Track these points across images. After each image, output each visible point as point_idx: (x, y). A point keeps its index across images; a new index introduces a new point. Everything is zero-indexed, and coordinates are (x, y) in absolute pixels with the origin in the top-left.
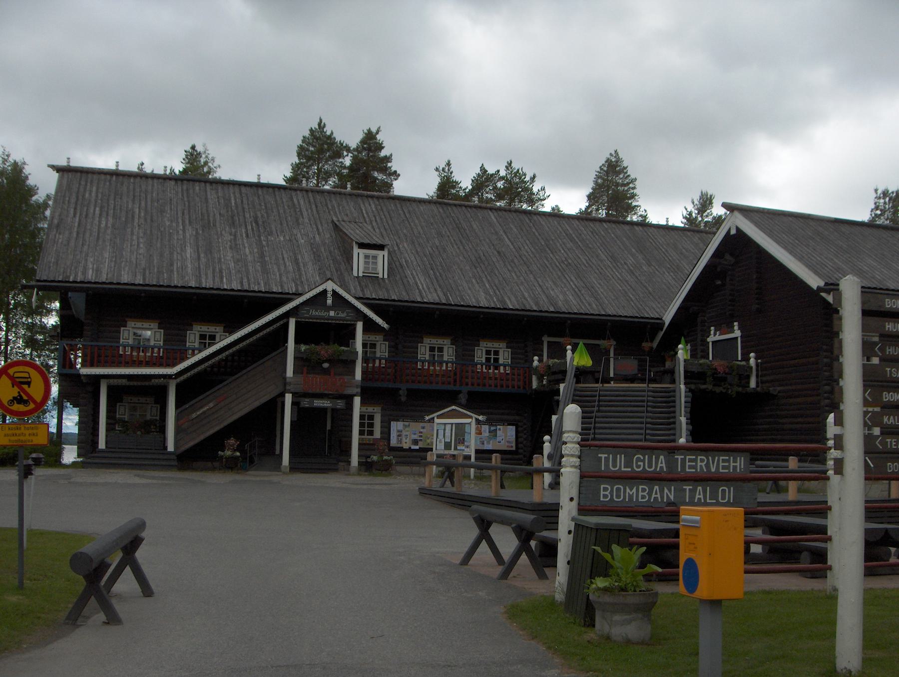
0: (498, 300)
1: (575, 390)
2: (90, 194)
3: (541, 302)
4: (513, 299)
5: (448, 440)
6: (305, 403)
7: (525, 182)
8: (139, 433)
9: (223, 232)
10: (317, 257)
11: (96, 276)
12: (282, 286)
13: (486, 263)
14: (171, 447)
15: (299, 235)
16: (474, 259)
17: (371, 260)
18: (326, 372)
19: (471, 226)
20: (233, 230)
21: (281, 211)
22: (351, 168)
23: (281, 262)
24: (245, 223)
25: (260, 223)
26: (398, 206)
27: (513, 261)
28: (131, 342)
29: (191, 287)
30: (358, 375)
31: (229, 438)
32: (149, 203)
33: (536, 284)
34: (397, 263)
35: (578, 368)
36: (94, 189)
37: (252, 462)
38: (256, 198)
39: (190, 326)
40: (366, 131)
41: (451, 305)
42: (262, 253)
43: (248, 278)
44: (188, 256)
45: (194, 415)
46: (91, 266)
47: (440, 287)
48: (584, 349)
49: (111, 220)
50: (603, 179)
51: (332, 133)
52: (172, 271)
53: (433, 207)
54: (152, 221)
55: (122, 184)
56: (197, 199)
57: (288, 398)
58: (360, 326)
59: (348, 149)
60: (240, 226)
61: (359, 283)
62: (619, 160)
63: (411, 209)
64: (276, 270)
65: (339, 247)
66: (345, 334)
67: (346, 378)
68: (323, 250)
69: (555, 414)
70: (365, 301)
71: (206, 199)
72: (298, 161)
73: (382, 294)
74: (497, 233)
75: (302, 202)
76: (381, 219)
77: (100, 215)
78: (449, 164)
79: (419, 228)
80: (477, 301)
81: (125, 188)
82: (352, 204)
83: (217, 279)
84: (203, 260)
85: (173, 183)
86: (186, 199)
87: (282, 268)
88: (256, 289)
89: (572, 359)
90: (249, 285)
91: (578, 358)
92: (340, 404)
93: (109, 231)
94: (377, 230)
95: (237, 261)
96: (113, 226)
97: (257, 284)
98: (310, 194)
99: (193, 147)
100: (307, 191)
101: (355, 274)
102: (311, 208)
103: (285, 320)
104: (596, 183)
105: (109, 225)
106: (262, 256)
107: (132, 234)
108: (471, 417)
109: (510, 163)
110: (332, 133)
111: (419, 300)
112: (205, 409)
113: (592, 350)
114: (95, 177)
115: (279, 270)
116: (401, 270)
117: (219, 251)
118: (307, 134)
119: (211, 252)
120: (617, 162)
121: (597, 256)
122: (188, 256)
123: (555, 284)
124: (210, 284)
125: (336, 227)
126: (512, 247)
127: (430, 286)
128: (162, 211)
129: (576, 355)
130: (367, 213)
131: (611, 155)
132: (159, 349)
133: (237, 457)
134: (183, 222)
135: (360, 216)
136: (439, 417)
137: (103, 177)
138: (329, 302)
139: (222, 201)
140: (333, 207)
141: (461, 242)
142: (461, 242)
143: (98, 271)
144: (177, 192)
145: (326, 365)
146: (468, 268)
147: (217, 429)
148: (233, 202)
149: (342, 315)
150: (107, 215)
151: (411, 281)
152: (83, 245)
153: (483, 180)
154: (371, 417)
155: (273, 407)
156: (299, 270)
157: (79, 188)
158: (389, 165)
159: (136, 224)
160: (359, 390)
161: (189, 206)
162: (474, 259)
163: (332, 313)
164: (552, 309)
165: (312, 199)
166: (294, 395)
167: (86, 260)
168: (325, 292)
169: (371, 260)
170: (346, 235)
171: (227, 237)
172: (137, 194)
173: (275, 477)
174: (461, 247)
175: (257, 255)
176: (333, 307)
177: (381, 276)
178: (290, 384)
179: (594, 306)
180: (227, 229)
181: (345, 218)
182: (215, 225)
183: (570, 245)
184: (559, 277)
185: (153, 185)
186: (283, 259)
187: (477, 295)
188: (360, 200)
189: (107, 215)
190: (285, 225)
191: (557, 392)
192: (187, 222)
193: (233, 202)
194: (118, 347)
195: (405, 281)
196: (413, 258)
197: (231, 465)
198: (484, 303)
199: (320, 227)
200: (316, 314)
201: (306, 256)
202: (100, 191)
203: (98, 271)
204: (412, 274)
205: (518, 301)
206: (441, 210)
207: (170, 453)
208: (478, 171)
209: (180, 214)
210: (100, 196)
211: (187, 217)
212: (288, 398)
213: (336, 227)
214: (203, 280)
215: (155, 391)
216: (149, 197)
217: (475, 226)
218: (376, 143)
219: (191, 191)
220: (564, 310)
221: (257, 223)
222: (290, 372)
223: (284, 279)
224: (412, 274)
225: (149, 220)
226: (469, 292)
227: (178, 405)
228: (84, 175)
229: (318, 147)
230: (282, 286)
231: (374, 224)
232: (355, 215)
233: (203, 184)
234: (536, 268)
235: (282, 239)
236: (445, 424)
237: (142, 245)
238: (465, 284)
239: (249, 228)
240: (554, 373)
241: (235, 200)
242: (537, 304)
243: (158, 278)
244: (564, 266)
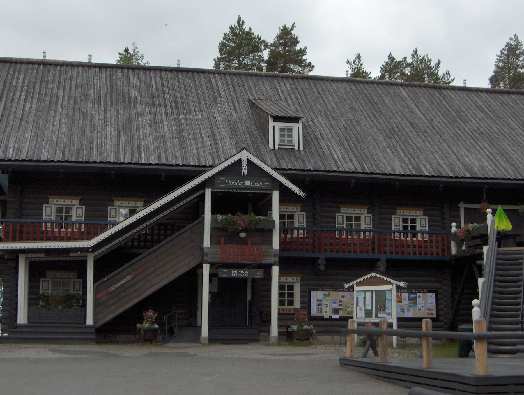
0: (414, 168)
1: (498, 254)
2: (17, 81)
3: (457, 169)
4: (428, 166)
5: (369, 308)
6: (223, 273)
7: (431, 68)
8: (60, 307)
9: (144, 112)
10: (234, 132)
11: (17, 155)
12: (199, 160)
13: (400, 134)
14: (90, 321)
15: (217, 113)
16: (387, 130)
17: (286, 133)
18: (243, 241)
19: (384, 101)
20: (153, 110)
21: (200, 92)
22: (268, 62)
23: (199, 137)
24: (165, 103)
25: (179, 103)
26: (312, 85)
27: (425, 131)
28: (53, 218)
29: (109, 163)
30: (276, 245)
31: (147, 310)
32: (73, 88)
33: (450, 152)
34: (312, 136)
35: (499, 233)
36: (22, 76)
37: (171, 331)
38: (176, 82)
39: (111, 202)
40: (281, 28)
41: (367, 173)
42: (180, 129)
43: (166, 152)
44: (108, 134)
45: (112, 288)
46: (12, 145)
47: (355, 156)
48: (503, 213)
49: (35, 103)
50: (504, 63)
51: (250, 29)
52: (91, 148)
53: (346, 85)
54: (75, 103)
55: (49, 72)
56: (120, 83)
57: (206, 269)
58: (276, 195)
59: (266, 46)
60: (160, 106)
61: (276, 155)
62: (518, 44)
63: (325, 87)
64: (194, 145)
65: (255, 123)
66: (260, 203)
67: (264, 247)
68: (240, 126)
69: (481, 276)
70: (282, 172)
71: (128, 83)
72: (220, 57)
73: (299, 165)
74: (408, 107)
75: (220, 84)
76: (296, 97)
77: (26, 99)
78: (359, 57)
79: (333, 104)
80: (393, 169)
81: (51, 75)
82: (267, 84)
83: (135, 155)
84: (122, 137)
85: (97, 70)
86: (109, 84)
87: (200, 143)
88: (174, 163)
89: (493, 222)
90: (167, 159)
91: (497, 221)
92: (259, 274)
93: (33, 114)
94: (292, 107)
95: (155, 138)
96: (37, 109)
97: (175, 157)
98: (228, 77)
99: (127, 50)
100: (225, 74)
101: (271, 147)
102: (229, 89)
103: (201, 192)
104: (497, 66)
105: (34, 108)
106: (180, 132)
107: (55, 115)
108: (392, 284)
109: (416, 52)
110: (250, 29)
111: (335, 169)
112: (124, 281)
113: (511, 215)
114: (23, 66)
115: (196, 145)
116: (316, 143)
117: (139, 128)
118: (227, 31)
119: (131, 130)
120: (517, 45)
121: (508, 125)
122: (108, 134)
123: (469, 151)
124: (128, 159)
125: (253, 105)
126: (424, 119)
127: (346, 156)
128: (86, 95)
129: (496, 218)
130: (282, 92)
131: (511, 39)
132: (80, 225)
133: (155, 330)
134: (105, 103)
135: (278, 96)
136: (358, 284)
137: (30, 66)
138: (245, 171)
139: (143, 84)
140: (249, 87)
141: (374, 116)
142: (374, 116)
143: (19, 150)
144: (100, 79)
145: (243, 235)
146: (382, 138)
147: (136, 301)
148: (154, 85)
149: (258, 184)
150: (32, 99)
151: (327, 152)
152: (6, 126)
153: (392, 67)
154: (291, 287)
155: (193, 277)
156: (216, 144)
157: (7, 77)
158: (304, 57)
159: (59, 106)
160: (277, 259)
161: (111, 90)
162: (387, 130)
163: (248, 183)
164: (468, 175)
165: (229, 82)
166: (212, 265)
167: (8, 140)
168: (240, 161)
169: (286, 133)
170: (262, 110)
171: (147, 116)
172: (62, 80)
173: (193, 349)
174: (375, 121)
175: (175, 132)
176: (249, 176)
177: (296, 148)
178: (207, 254)
179: (510, 171)
180: (148, 109)
181: (262, 97)
182: (135, 106)
183: (480, 115)
184: (473, 145)
185: (78, 73)
186: (201, 135)
187: (392, 163)
188: (275, 81)
189: (32, 99)
190: (203, 104)
191: (480, 256)
192: (109, 104)
193: (154, 85)
194: (40, 224)
195: (321, 153)
196: (327, 131)
197: (150, 338)
198: (399, 170)
199: (237, 105)
200: (231, 184)
201: (223, 132)
202: (27, 78)
203: (19, 150)
204: (327, 146)
205: (433, 168)
206: (353, 88)
207: (90, 327)
208: (387, 59)
209: (102, 97)
210: (26, 83)
211: (109, 99)
212: (206, 269)
213: (253, 105)
214: (122, 156)
215: (73, 264)
216: (74, 83)
217: (387, 101)
218: (291, 38)
219: (114, 77)
220: (480, 175)
221: (176, 103)
222: (207, 243)
223: (201, 153)
224: (327, 146)
226: (384, 161)
228: (13, 65)
229: (239, 42)
230: (199, 160)
231: (289, 101)
232: (271, 94)
233: (126, 70)
234: (449, 137)
235: (200, 117)
236: (365, 292)
237: (63, 126)
238: (380, 154)
239: (169, 107)
240: (474, 238)
241: (156, 83)
242: (452, 170)
243: (77, 155)
244: (477, 135)
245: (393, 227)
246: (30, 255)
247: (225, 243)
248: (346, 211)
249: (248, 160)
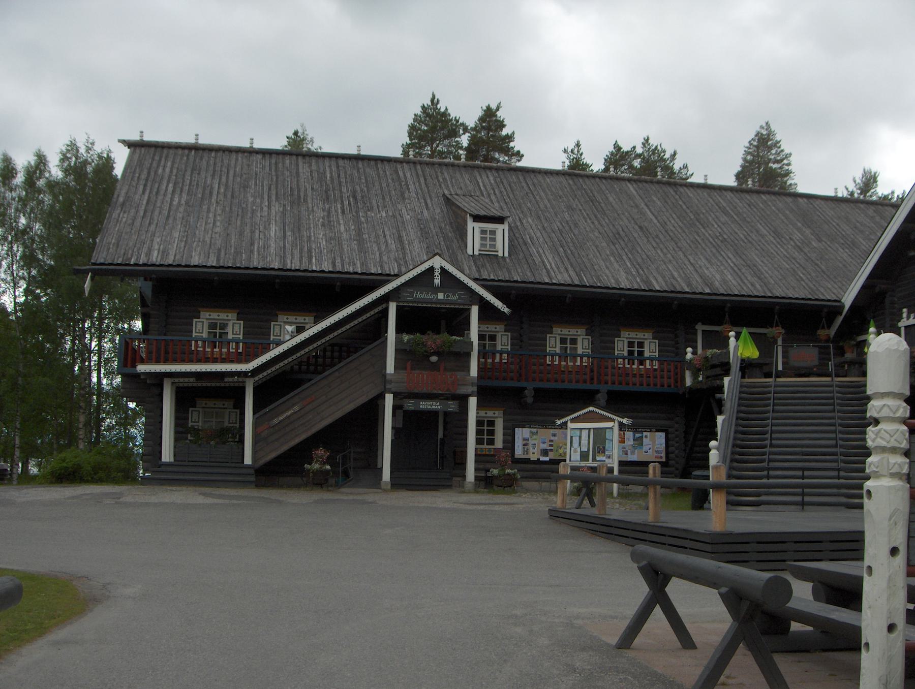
0: (642, 280)
1: (741, 386)
2: (164, 170)
3: (694, 283)
4: (660, 279)
6: (410, 405)
7: (665, 160)
8: (212, 443)
9: (315, 208)
10: (424, 233)
11: (162, 258)
12: (382, 267)
13: (626, 239)
14: (248, 460)
15: (404, 211)
16: (611, 235)
17: (488, 236)
18: (434, 367)
19: (607, 198)
20: (327, 206)
21: (384, 185)
22: (468, 149)
23: (382, 239)
24: (342, 197)
25: (359, 198)
26: (521, 178)
27: (657, 236)
28: (205, 335)
29: (273, 269)
30: (474, 372)
31: (317, 448)
32: (231, 178)
33: (687, 262)
34: (520, 240)
35: (743, 360)
36: (169, 164)
37: (346, 474)
38: (355, 172)
39: (275, 318)
40: (485, 108)
41: (586, 286)
42: (360, 230)
43: (342, 258)
44: (272, 234)
45: (276, 421)
46: (157, 247)
47: (572, 266)
48: (749, 338)
49: (184, 196)
50: (753, 156)
51: (446, 109)
52: (252, 252)
53: (562, 179)
54: (233, 197)
55: (201, 159)
56: (287, 173)
57: (389, 399)
59: (466, 130)
60: (335, 201)
61: (475, 263)
62: (770, 134)
63: (536, 181)
64: (376, 249)
65: (451, 223)
66: (455, 320)
67: (459, 375)
68: (432, 227)
69: (721, 413)
70: (482, 282)
71: (298, 174)
72: (409, 142)
73: (502, 275)
74: (637, 206)
75: (408, 175)
76: (501, 192)
77: (174, 191)
78: (578, 145)
79: (546, 201)
80: (617, 281)
81: (204, 163)
82: (466, 177)
83: (305, 260)
84: (290, 239)
85: (260, 156)
86: (274, 173)
87: (383, 247)
88: (351, 270)
89: (736, 348)
90: (343, 265)
91: (741, 347)
92: (452, 406)
93: (182, 209)
94: (496, 204)
95: (329, 240)
96: (187, 203)
97: (353, 264)
98: (418, 167)
99: (296, 133)
100: (414, 163)
101: (470, 252)
102: (419, 182)
103: (384, 306)
104: (745, 160)
105: (183, 202)
106: (359, 232)
107: (209, 211)
108: (613, 420)
109: (647, 140)
110: (446, 109)
111: (547, 281)
112: (289, 413)
113: (757, 339)
114: (171, 151)
115: (379, 249)
116: (524, 248)
117: (310, 228)
118: (419, 111)
119: (299, 230)
120: (768, 135)
121: (757, 232)
122: (272, 234)
123: (709, 262)
124: (296, 265)
125: (448, 201)
126: (656, 221)
127: (561, 265)
128: (245, 187)
129: (741, 343)
130: (484, 186)
131: (762, 127)
132: (237, 343)
133: (327, 472)
134: (269, 197)
135: (480, 191)
136: (573, 421)
137: (180, 152)
138: (437, 281)
139: (315, 175)
140: (445, 179)
141: (596, 217)
142: (596, 217)
143: (165, 253)
144: (264, 168)
145: (434, 359)
146: (604, 244)
147: (304, 437)
148: (328, 175)
149: (454, 298)
150: (181, 192)
151: (537, 260)
152: (150, 224)
153: (618, 157)
154: (491, 423)
155: (373, 408)
156: (403, 248)
157: (151, 164)
158: (512, 144)
159: (213, 200)
160: (475, 389)
161: (277, 181)
162: (611, 235)
163: (441, 296)
164: (707, 291)
165: (420, 173)
166: (396, 395)
167: (152, 241)
168: (431, 270)
169: (488, 236)
170: (459, 207)
171: (320, 213)
172: (218, 169)
173: (371, 496)
174: (596, 222)
175: (353, 233)
176: (442, 288)
177: (500, 254)
178: (391, 382)
179: (758, 286)
180: (320, 205)
181: (459, 192)
182: (305, 201)
183: (724, 218)
184: (714, 255)
185: (237, 160)
186: (385, 236)
187: (617, 275)
188: (476, 173)
189: (181, 192)
190: (388, 199)
191: (720, 389)
192: (274, 198)
193: (328, 175)
194: (189, 342)
195: (530, 261)
196: (539, 234)
197: (320, 482)
198: (625, 284)
199: (429, 201)
200: (421, 296)
201: (412, 234)
202: (176, 166)
203: (165, 253)
204: (538, 252)
205: (666, 282)
206: (571, 182)
207: (248, 467)
208: (612, 149)
209: (266, 188)
210: (175, 171)
211: (274, 192)
212: (389, 399)
213: (448, 201)
214: (289, 262)
215: (227, 391)
216: (231, 173)
217: (611, 199)
218: (497, 121)
219: (280, 165)
220: (722, 291)
221: (355, 197)
222: (390, 368)
223: (385, 258)
224: (538, 252)
225: (229, 196)
226: (607, 272)
227: (255, 411)
228: (159, 150)
229: (433, 125)
230: (382, 267)
231: (493, 197)
232: (471, 188)
233: (294, 157)
234: (685, 244)
235: (384, 215)
236: (581, 429)
237: (218, 224)
238: (602, 263)
239: (346, 203)
240: (714, 366)
241: (331, 173)
242: (689, 285)
243: (235, 259)
244: (719, 243)
245: (616, 352)
246: (176, 380)
247: (412, 369)
248: (560, 332)
249: (441, 268)
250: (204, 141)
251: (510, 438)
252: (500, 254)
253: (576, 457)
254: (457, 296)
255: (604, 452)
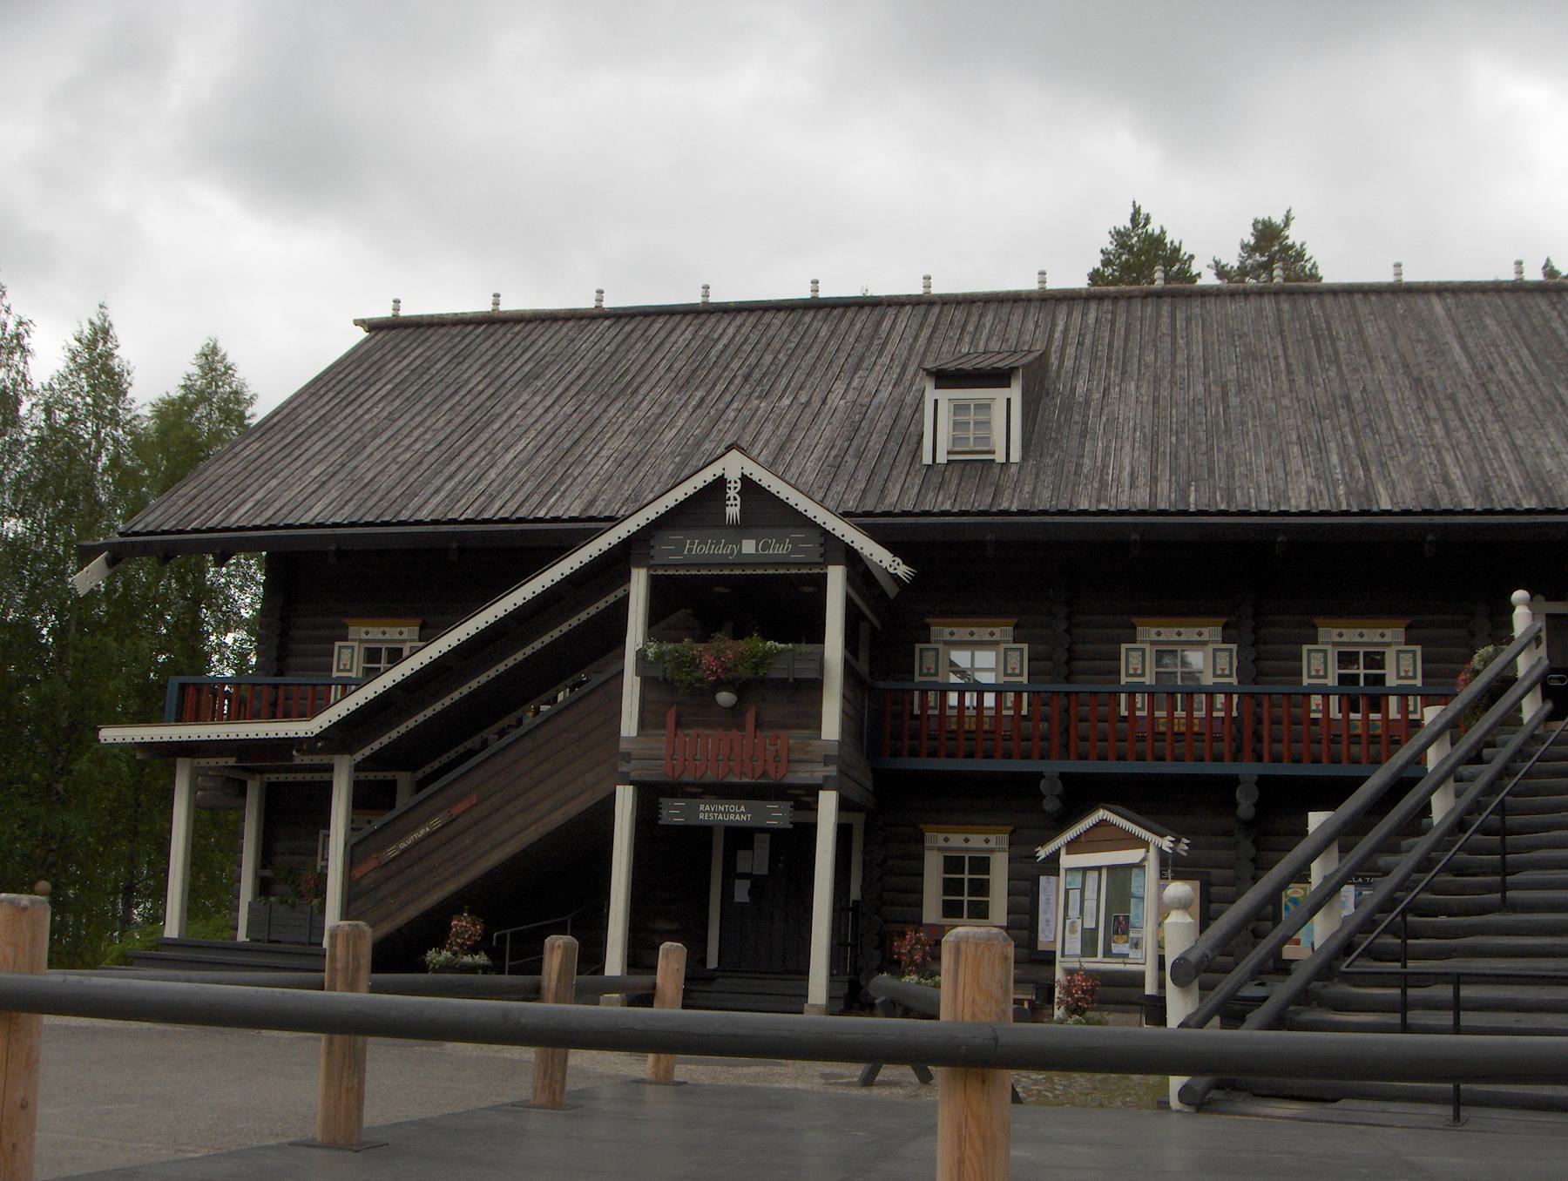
5: (1090, 924)
6: (673, 812)
17: (972, 417)
27: (1452, 398)
30: (831, 725)
45: (392, 852)
57: (625, 799)
58: (836, 577)
66: (787, 607)
67: (794, 737)
92: (777, 815)
101: (927, 460)
108: (1144, 844)
136: (1074, 846)
138: (733, 511)
145: (725, 698)
154: (982, 865)
160: (832, 770)
163: (749, 547)
168: (720, 483)
176: (747, 525)
177: (1000, 457)
178: (627, 757)
200: (697, 550)
217: (1370, 330)
222: (629, 725)
236: (1085, 870)
245: (1306, 681)
246: (203, 762)
247: (679, 725)
248: (1151, 634)
249: (744, 478)
250: (512, 303)
251: (1024, 901)
252: (1000, 457)
253: (1075, 944)
254: (788, 546)
255: (1125, 932)
